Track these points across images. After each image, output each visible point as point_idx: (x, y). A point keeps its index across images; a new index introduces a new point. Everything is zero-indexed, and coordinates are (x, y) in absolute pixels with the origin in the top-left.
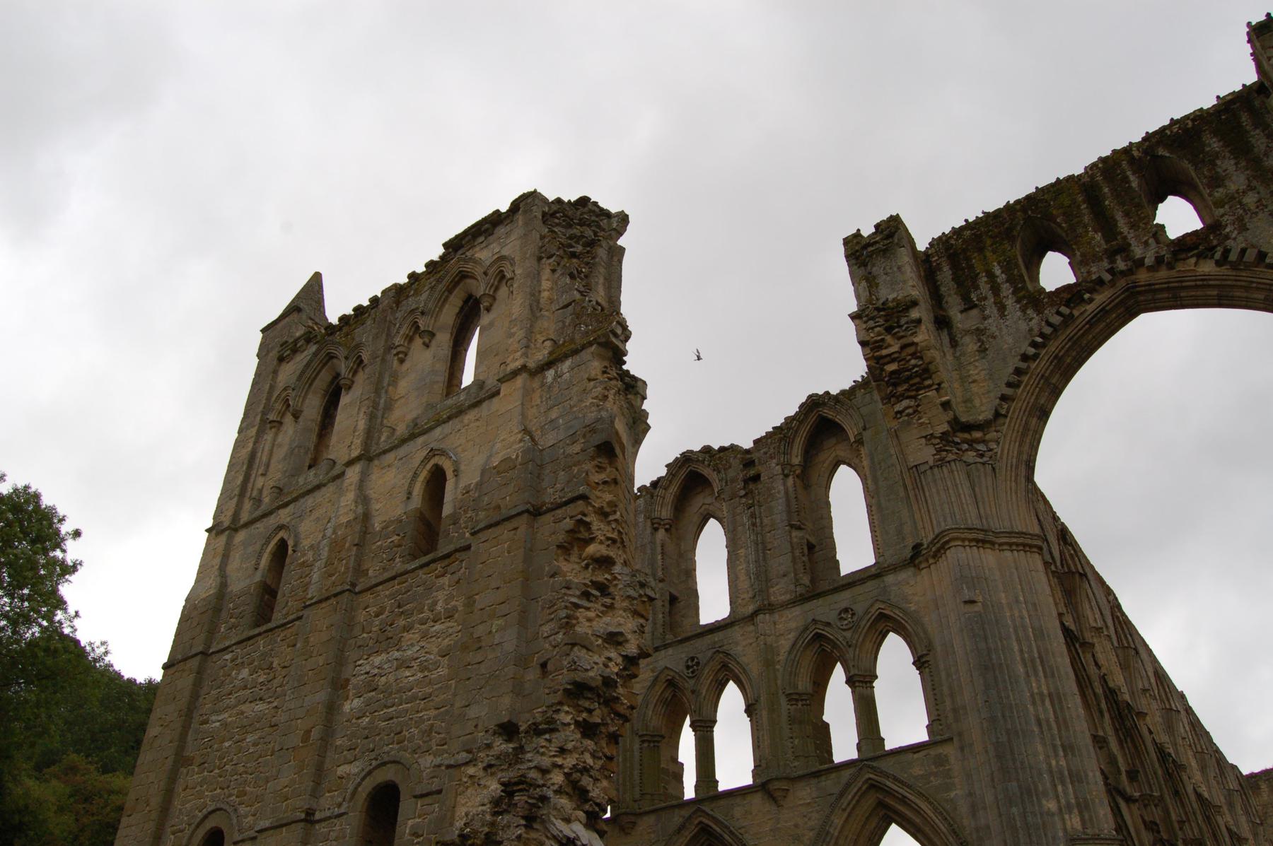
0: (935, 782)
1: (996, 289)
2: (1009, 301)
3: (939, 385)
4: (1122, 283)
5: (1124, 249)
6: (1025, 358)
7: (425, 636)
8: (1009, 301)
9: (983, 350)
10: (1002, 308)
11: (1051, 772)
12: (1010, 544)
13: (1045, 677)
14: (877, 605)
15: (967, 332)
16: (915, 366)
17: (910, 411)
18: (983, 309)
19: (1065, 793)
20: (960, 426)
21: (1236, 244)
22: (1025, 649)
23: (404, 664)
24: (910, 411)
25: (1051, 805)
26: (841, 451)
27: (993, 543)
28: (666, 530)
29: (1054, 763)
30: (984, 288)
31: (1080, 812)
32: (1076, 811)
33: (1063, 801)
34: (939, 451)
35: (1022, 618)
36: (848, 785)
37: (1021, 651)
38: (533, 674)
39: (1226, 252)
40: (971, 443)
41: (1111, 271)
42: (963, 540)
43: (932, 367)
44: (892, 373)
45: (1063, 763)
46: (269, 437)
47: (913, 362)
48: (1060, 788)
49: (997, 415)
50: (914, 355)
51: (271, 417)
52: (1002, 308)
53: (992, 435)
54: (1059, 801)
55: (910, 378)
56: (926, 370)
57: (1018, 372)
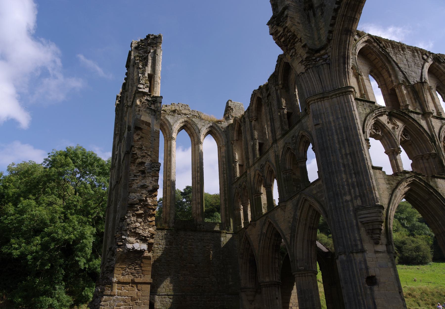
0: (319, 195)
3: (300, 39)
11: (348, 185)
12: (336, 95)
13: (349, 146)
14: (301, 132)
16: (289, 36)
17: (294, 54)
19: (355, 192)
20: (313, 51)
22: (340, 137)
24: (294, 54)
25: (348, 198)
27: (328, 97)
28: (255, 121)
29: (350, 181)
31: (361, 199)
32: (359, 198)
33: (353, 196)
34: (306, 66)
35: (339, 124)
36: (298, 201)
37: (338, 138)
40: (320, 57)
42: (314, 100)
43: (295, 33)
44: (283, 41)
45: (354, 180)
47: (288, 34)
48: (352, 191)
50: (288, 32)
54: (351, 196)
55: (290, 41)
56: (294, 35)
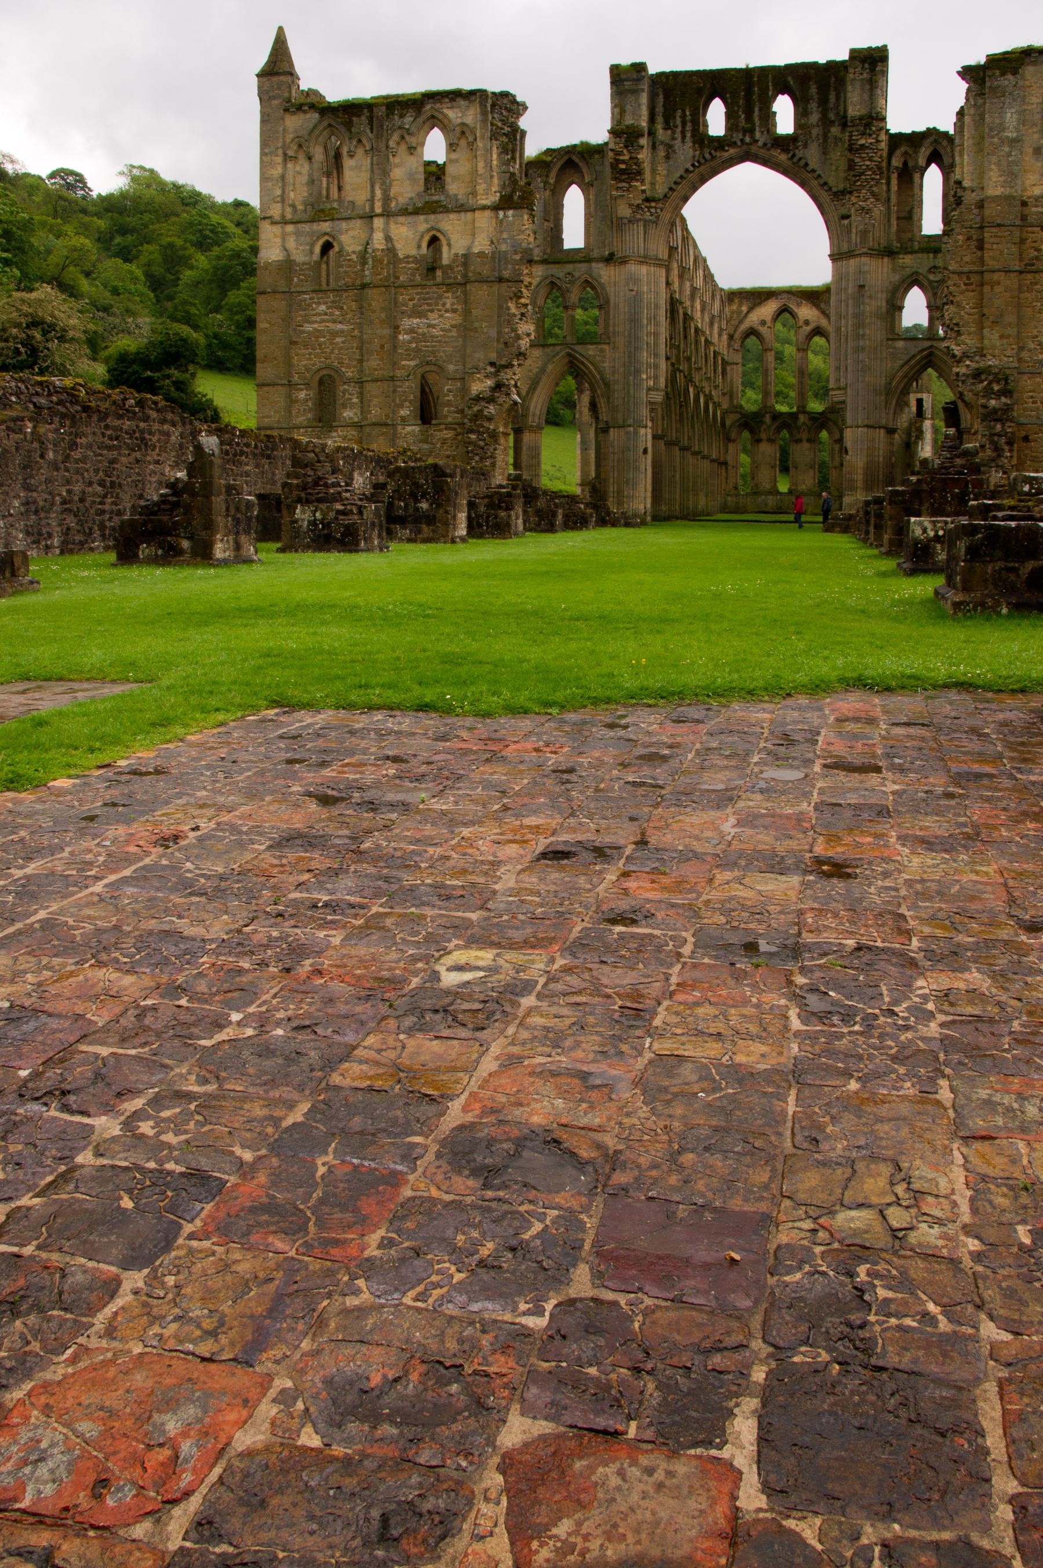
1: (684, 124)
2: (689, 135)
4: (745, 147)
5: (751, 131)
6: (687, 171)
7: (441, 316)
8: (689, 135)
9: (667, 157)
10: (684, 137)
15: (662, 143)
18: (674, 133)
20: (647, 200)
21: (799, 154)
23: (430, 326)
26: (576, 177)
30: (678, 121)
38: (502, 346)
39: (794, 156)
41: (742, 140)
46: (290, 165)
49: (665, 196)
51: (290, 153)
52: (684, 137)
53: (660, 205)
57: (681, 177)
